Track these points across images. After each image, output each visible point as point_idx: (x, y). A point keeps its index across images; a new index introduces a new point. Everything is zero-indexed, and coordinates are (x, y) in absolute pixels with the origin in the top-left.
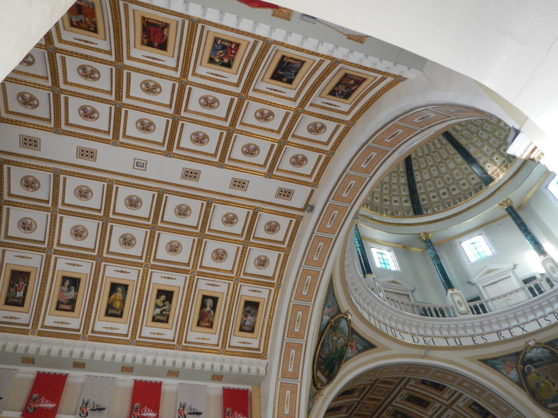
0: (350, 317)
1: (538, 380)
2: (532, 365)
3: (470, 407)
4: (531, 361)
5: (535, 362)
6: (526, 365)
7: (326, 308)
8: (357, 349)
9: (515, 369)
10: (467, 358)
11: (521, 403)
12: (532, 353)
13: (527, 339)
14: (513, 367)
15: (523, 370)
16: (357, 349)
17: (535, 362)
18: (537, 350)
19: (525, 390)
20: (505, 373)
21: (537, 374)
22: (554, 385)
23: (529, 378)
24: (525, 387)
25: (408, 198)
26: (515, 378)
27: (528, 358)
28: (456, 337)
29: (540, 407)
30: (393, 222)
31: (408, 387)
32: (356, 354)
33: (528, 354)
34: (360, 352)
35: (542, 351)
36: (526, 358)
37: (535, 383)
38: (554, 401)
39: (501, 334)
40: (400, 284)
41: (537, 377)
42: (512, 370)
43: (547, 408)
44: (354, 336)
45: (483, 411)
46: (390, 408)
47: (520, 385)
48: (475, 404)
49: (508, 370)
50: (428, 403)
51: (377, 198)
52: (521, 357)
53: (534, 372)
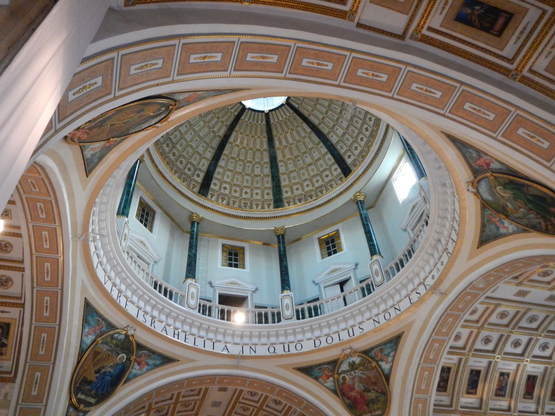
7: (502, 231)
34: (478, 151)
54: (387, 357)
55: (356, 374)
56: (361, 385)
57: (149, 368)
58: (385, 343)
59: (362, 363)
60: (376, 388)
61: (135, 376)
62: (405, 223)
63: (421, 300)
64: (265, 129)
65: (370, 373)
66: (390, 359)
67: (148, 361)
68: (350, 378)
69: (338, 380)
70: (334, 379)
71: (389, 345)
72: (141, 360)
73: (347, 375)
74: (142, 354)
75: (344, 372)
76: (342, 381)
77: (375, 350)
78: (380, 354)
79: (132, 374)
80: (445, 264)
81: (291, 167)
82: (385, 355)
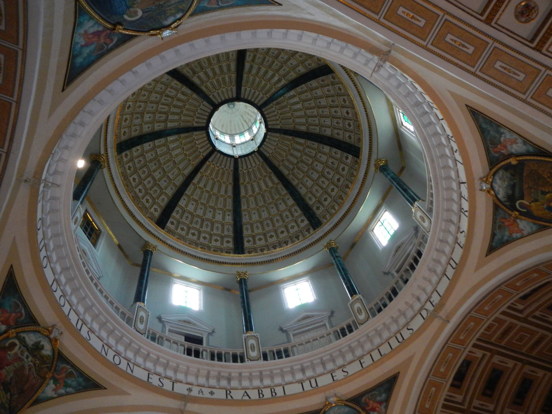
0: (333, 400)
1: (543, 205)
2: (518, 200)
4: (511, 199)
5: (513, 194)
6: (515, 205)
8: (380, 403)
9: (518, 221)
10: (477, 268)
12: (499, 191)
13: (477, 187)
14: (515, 221)
15: (521, 213)
16: (380, 403)
17: (513, 194)
18: (496, 183)
20: (519, 235)
21: (532, 202)
23: (536, 213)
25: (345, 154)
26: (532, 228)
27: (506, 199)
28: (449, 260)
30: (358, 189)
32: (386, 407)
33: (500, 196)
35: (500, 179)
36: (505, 201)
39: (463, 209)
40: (402, 243)
41: (538, 203)
42: (518, 225)
44: (364, 398)
49: (516, 229)
51: (333, 190)
52: (500, 205)
53: (530, 203)
54: (64, 386)
55: (26, 359)
56: (11, 375)
57: (78, 46)
58: (81, 374)
59: (45, 359)
60: (16, 396)
61: (76, 25)
62: (168, 318)
63: (159, 390)
64: (189, 124)
65: (34, 378)
66: (62, 391)
67: (92, 47)
68: (16, 354)
69: (8, 338)
70: (5, 332)
71: (81, 380)
72: (102, 37)
73: (20, 348)
74: (112, 40)
75: (23, 341)
76: (7, 345)
77: (68, 367)
78: (64, 375)
79: (86, 22)
80: (214, 396)
81: (149, 156)
82: (65, 382)
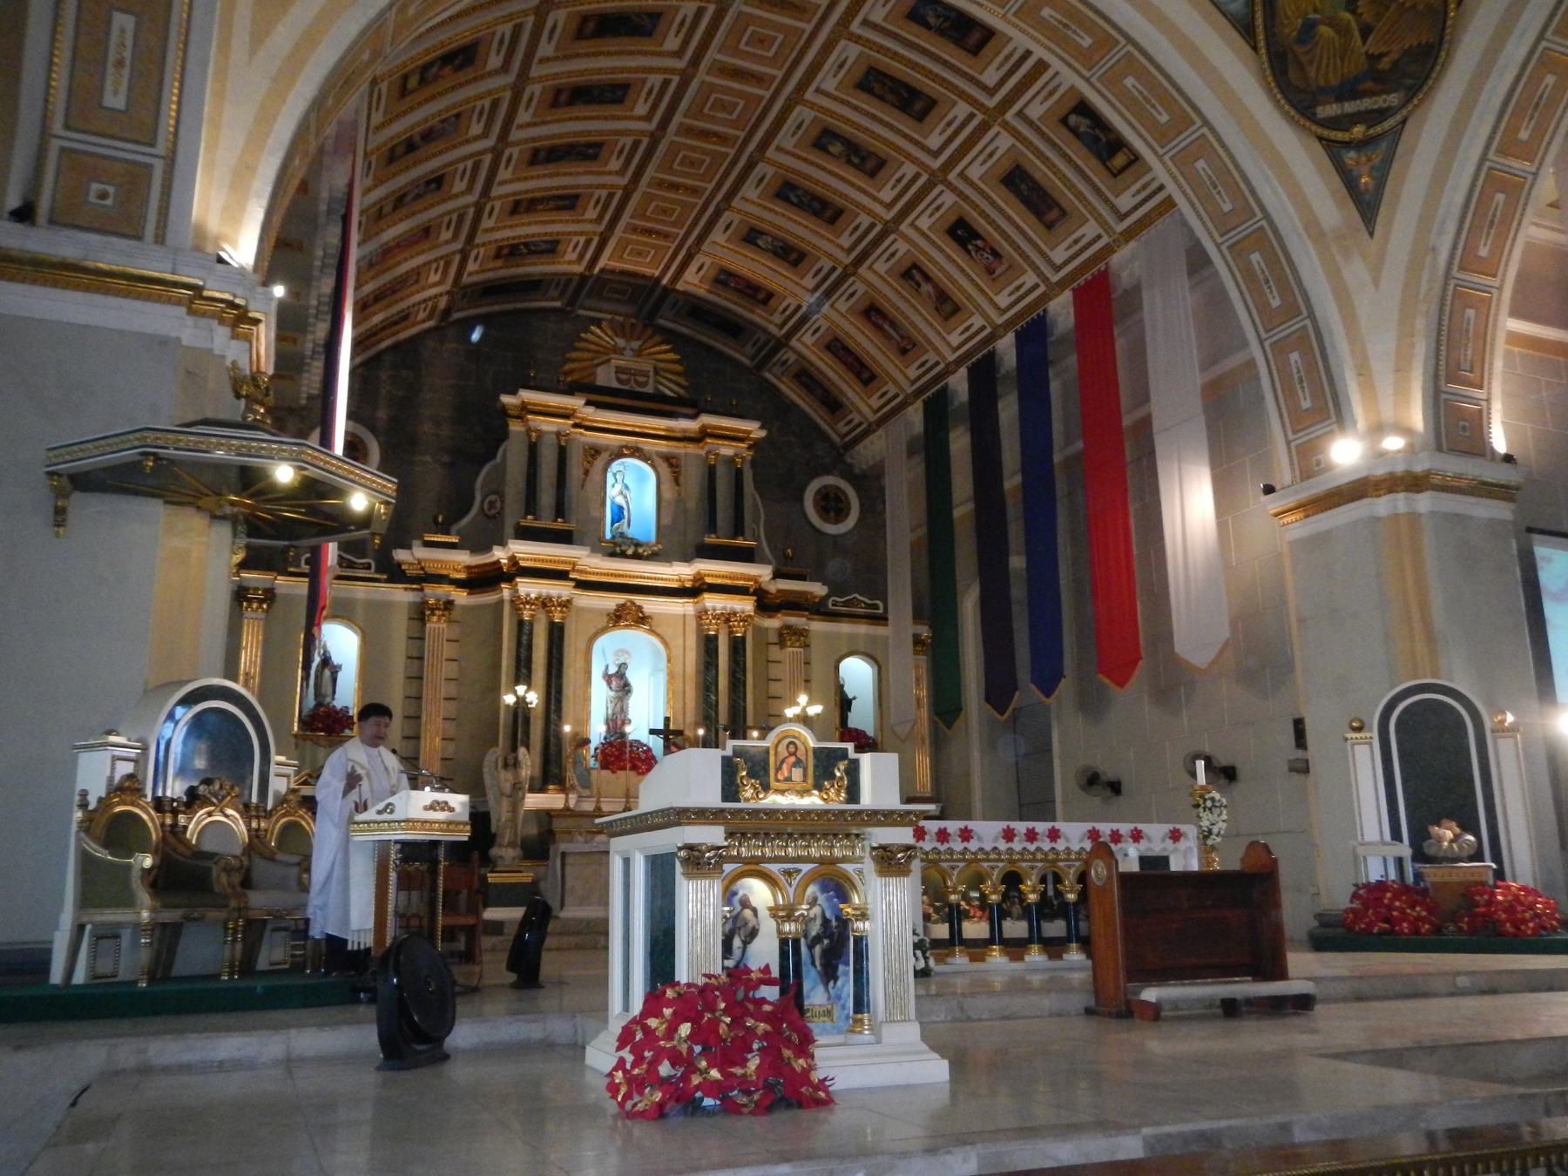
1: (1316, 11)
3: (1064, 121)
11: (1231, 100)
19: (1255, 48)
22: (1366, 32)
24: (1261, 37)
29: (1285, 115)
31: (855, 27)
37: (1300, 21)
38: (1347, 91)
43: (1312, 118)
45: (1104, 140)
46: (801, 113)
47: (1245, 28)
48: (1083, 108)
50: (931, 104)
